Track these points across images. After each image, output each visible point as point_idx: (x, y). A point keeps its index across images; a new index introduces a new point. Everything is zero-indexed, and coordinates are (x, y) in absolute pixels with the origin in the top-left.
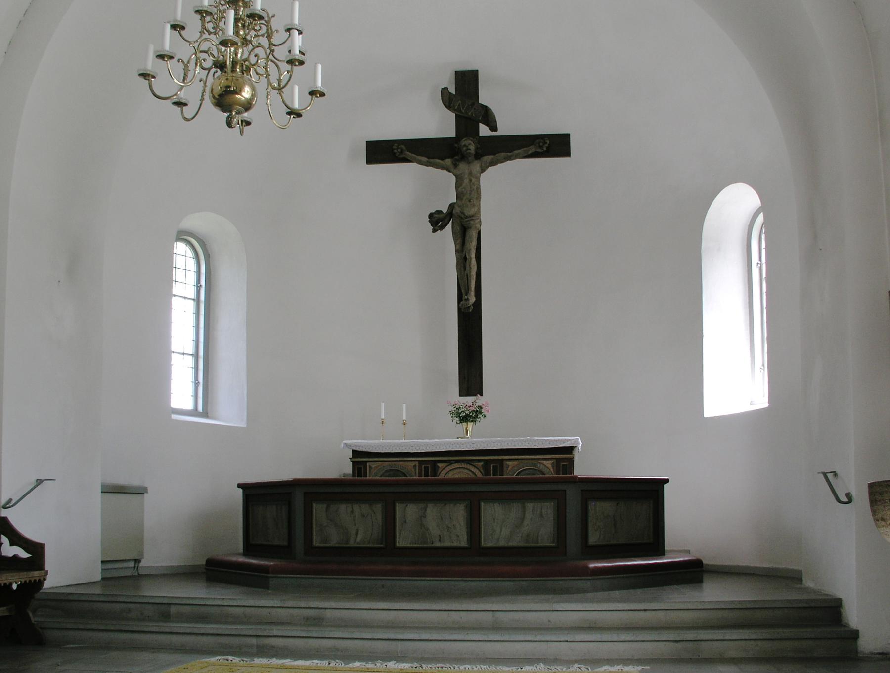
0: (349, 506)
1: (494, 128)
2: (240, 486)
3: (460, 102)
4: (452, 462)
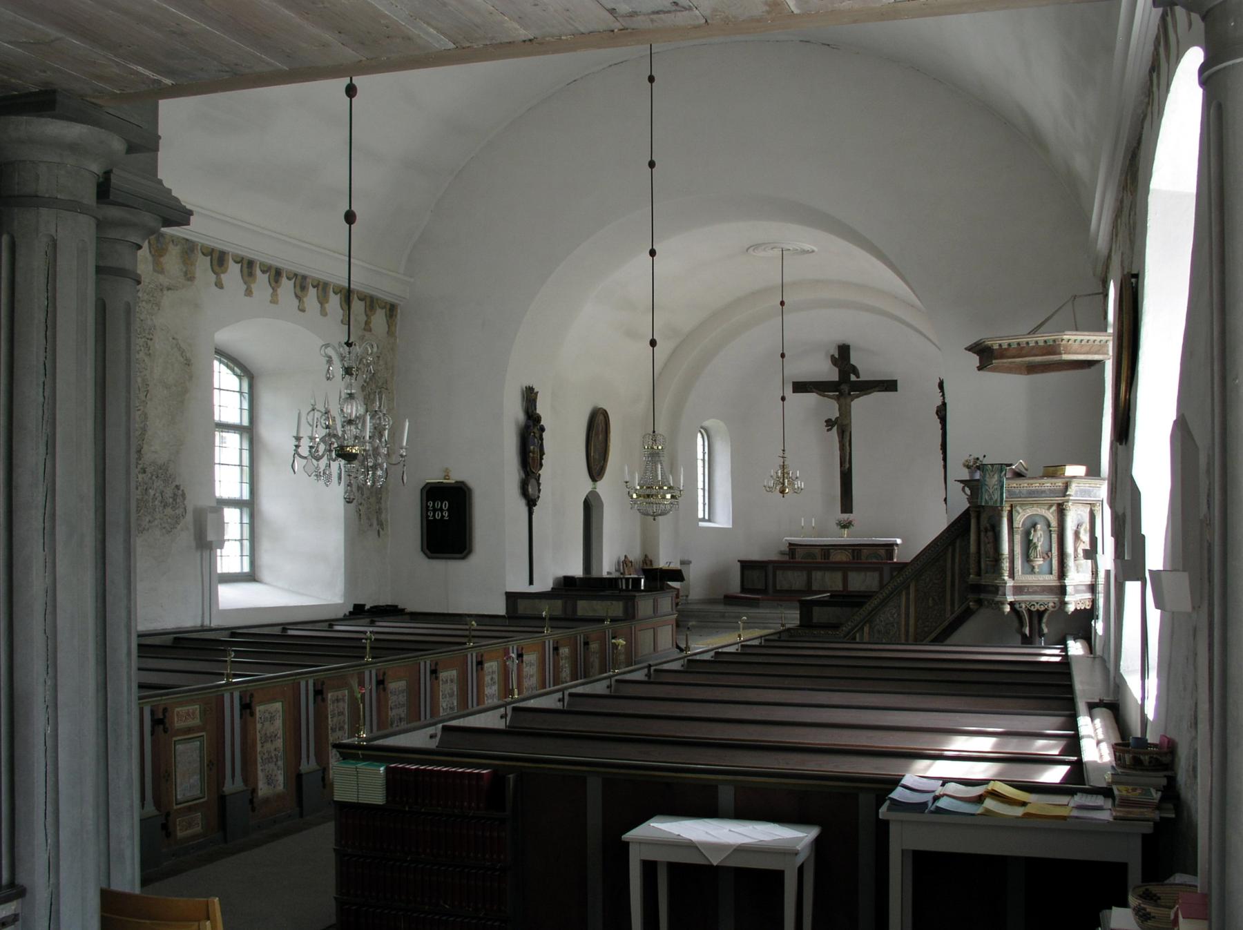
2: (739, 561)
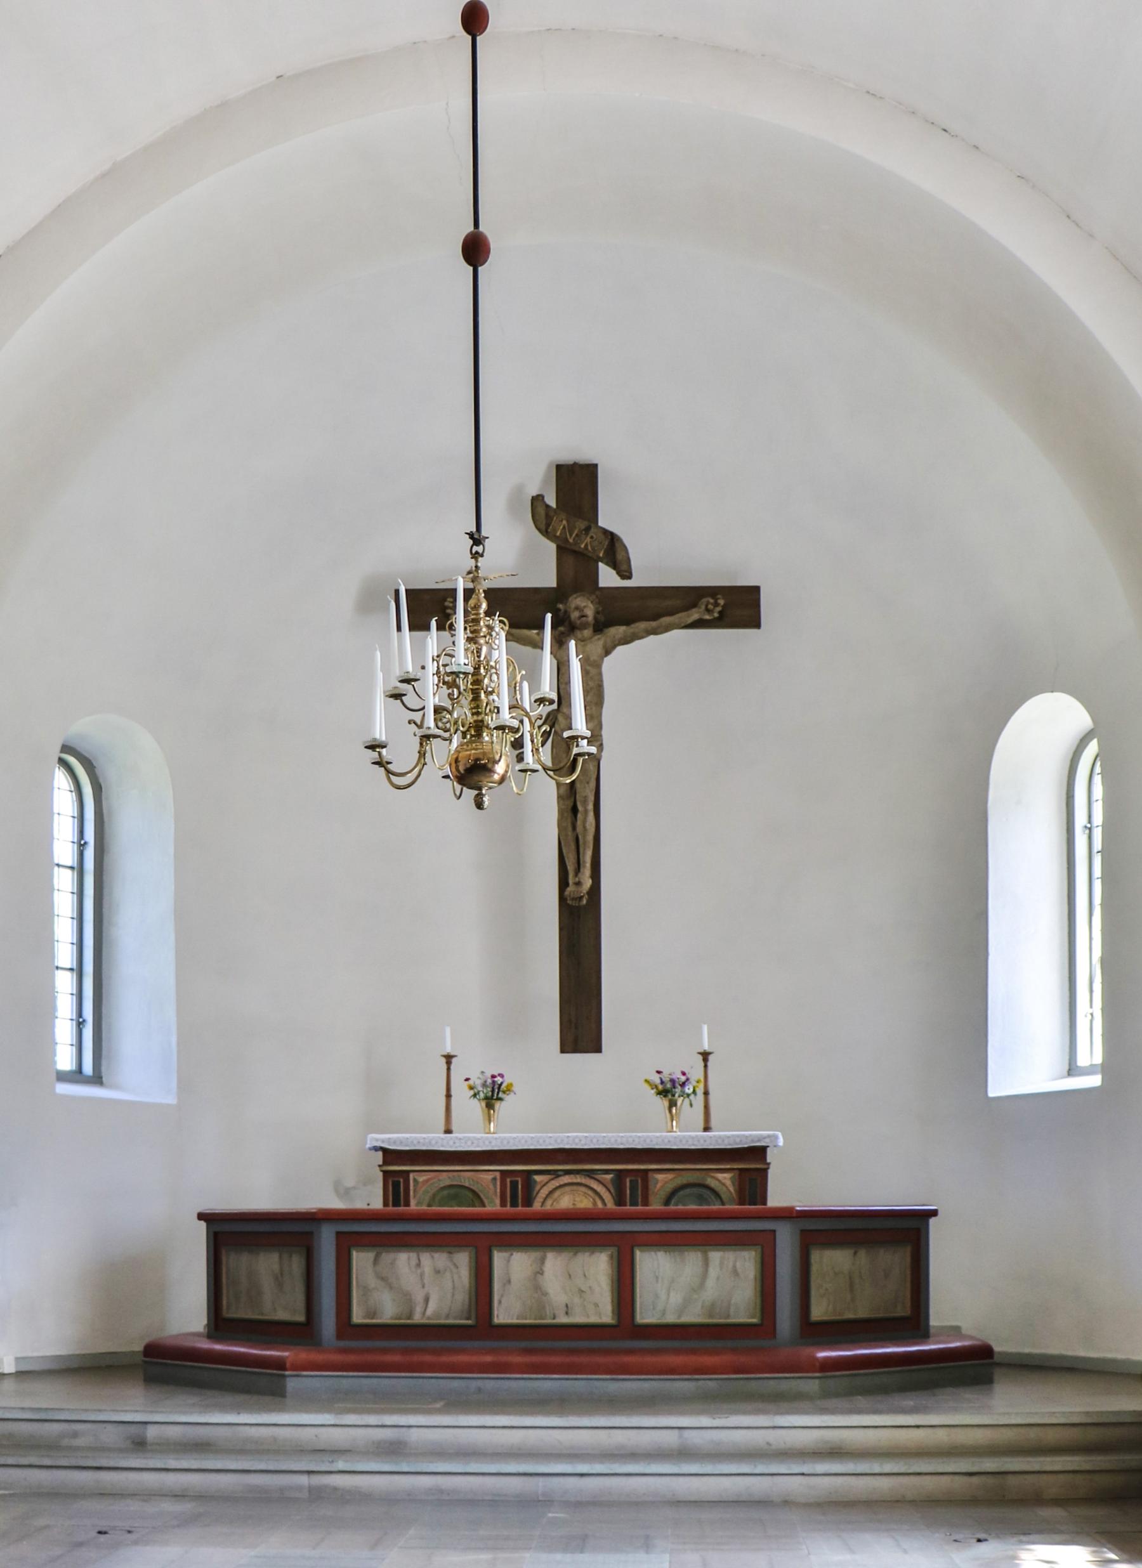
0: (413, 1255)
1: (626, 574)
2: (201, 1216)
3: (564, 522)
4: (560, 1173)
